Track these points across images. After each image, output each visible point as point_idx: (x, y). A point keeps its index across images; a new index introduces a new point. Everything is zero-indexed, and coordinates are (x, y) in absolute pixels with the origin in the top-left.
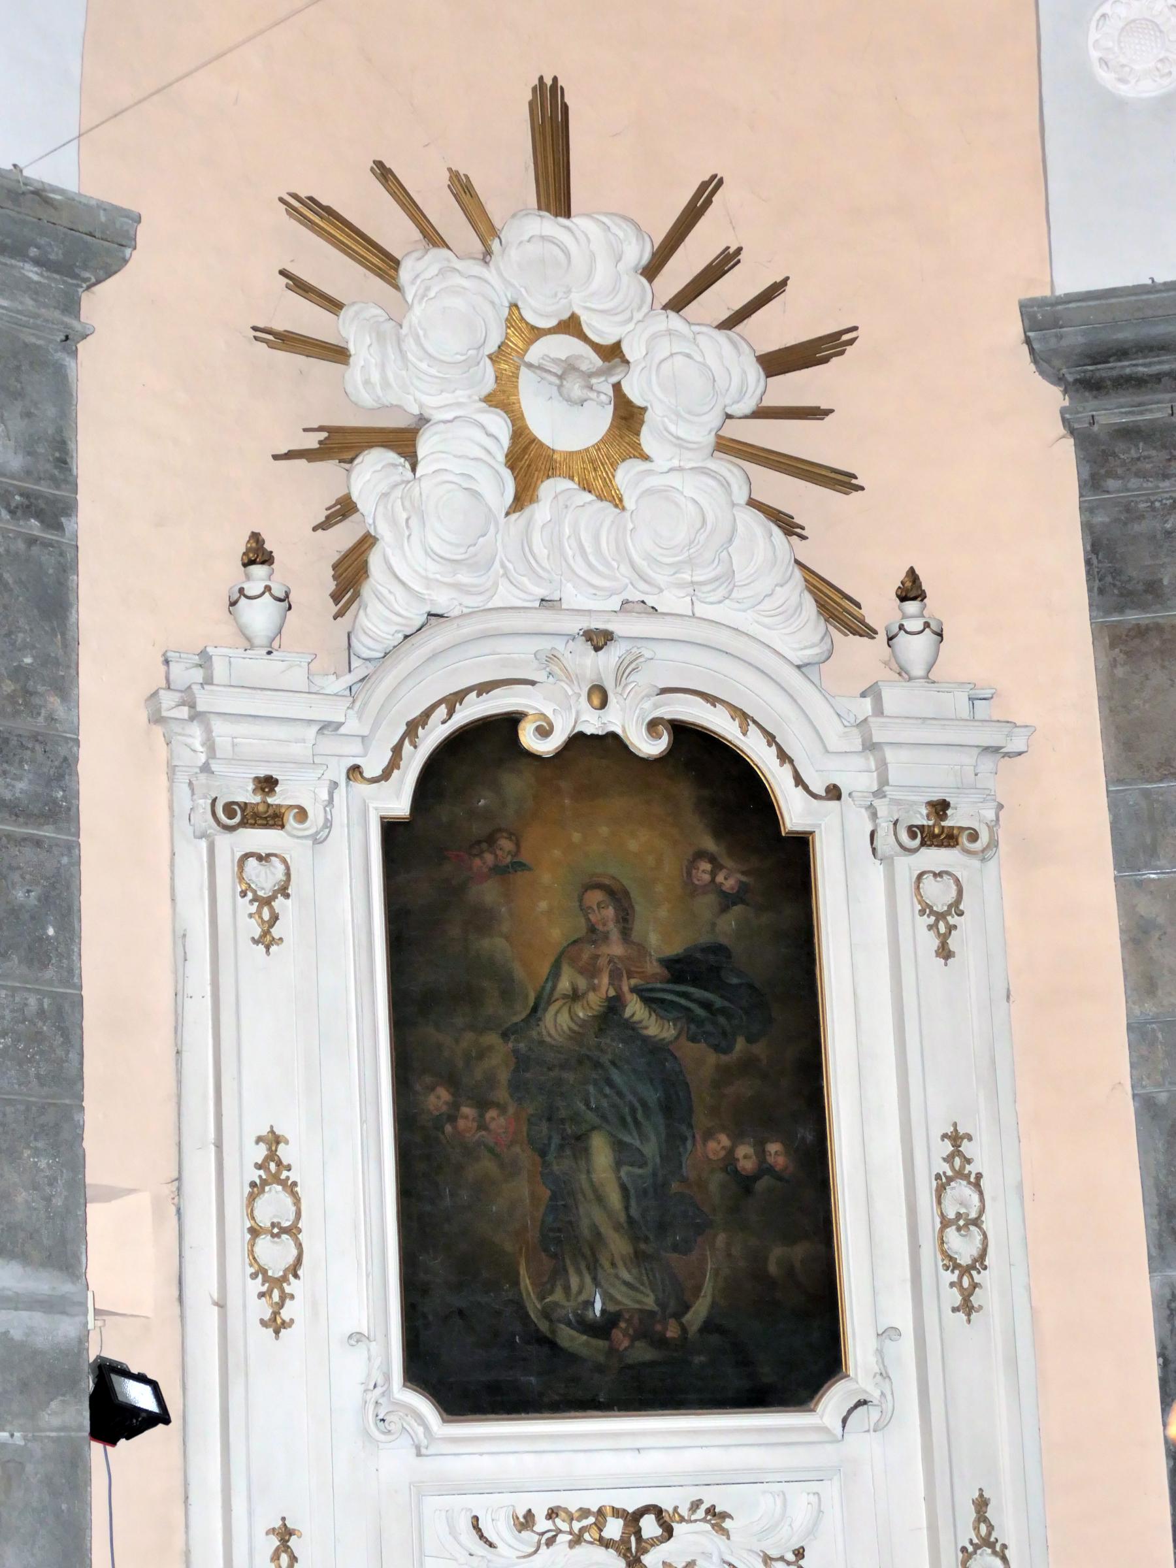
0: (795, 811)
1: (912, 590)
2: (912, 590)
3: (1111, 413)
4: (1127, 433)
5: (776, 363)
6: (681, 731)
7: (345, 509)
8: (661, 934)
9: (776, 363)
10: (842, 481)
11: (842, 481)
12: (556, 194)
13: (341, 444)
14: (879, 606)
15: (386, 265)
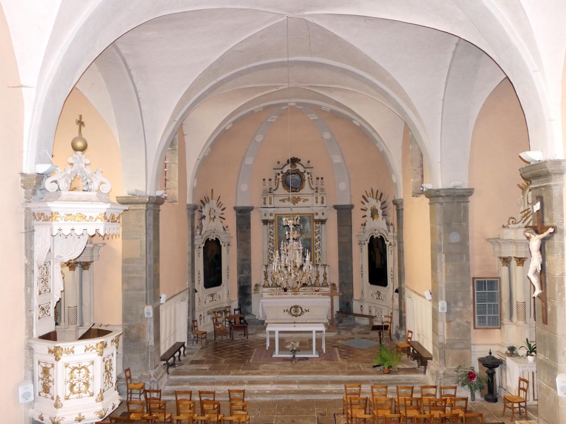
0: (221, 243)
1: (227, 227)
2: (227, 227)
3: (240, 214)
4: (241, 216)
5: (223, 210)
6: (217, 239)
7: (201, 223)
8: (215, 254)
9: (222, 210)
10: (224, 219)
11: (224, 219)
12: (212, 199)
13: (201, 219)
14: (225, 228)
15: (204, 205)
